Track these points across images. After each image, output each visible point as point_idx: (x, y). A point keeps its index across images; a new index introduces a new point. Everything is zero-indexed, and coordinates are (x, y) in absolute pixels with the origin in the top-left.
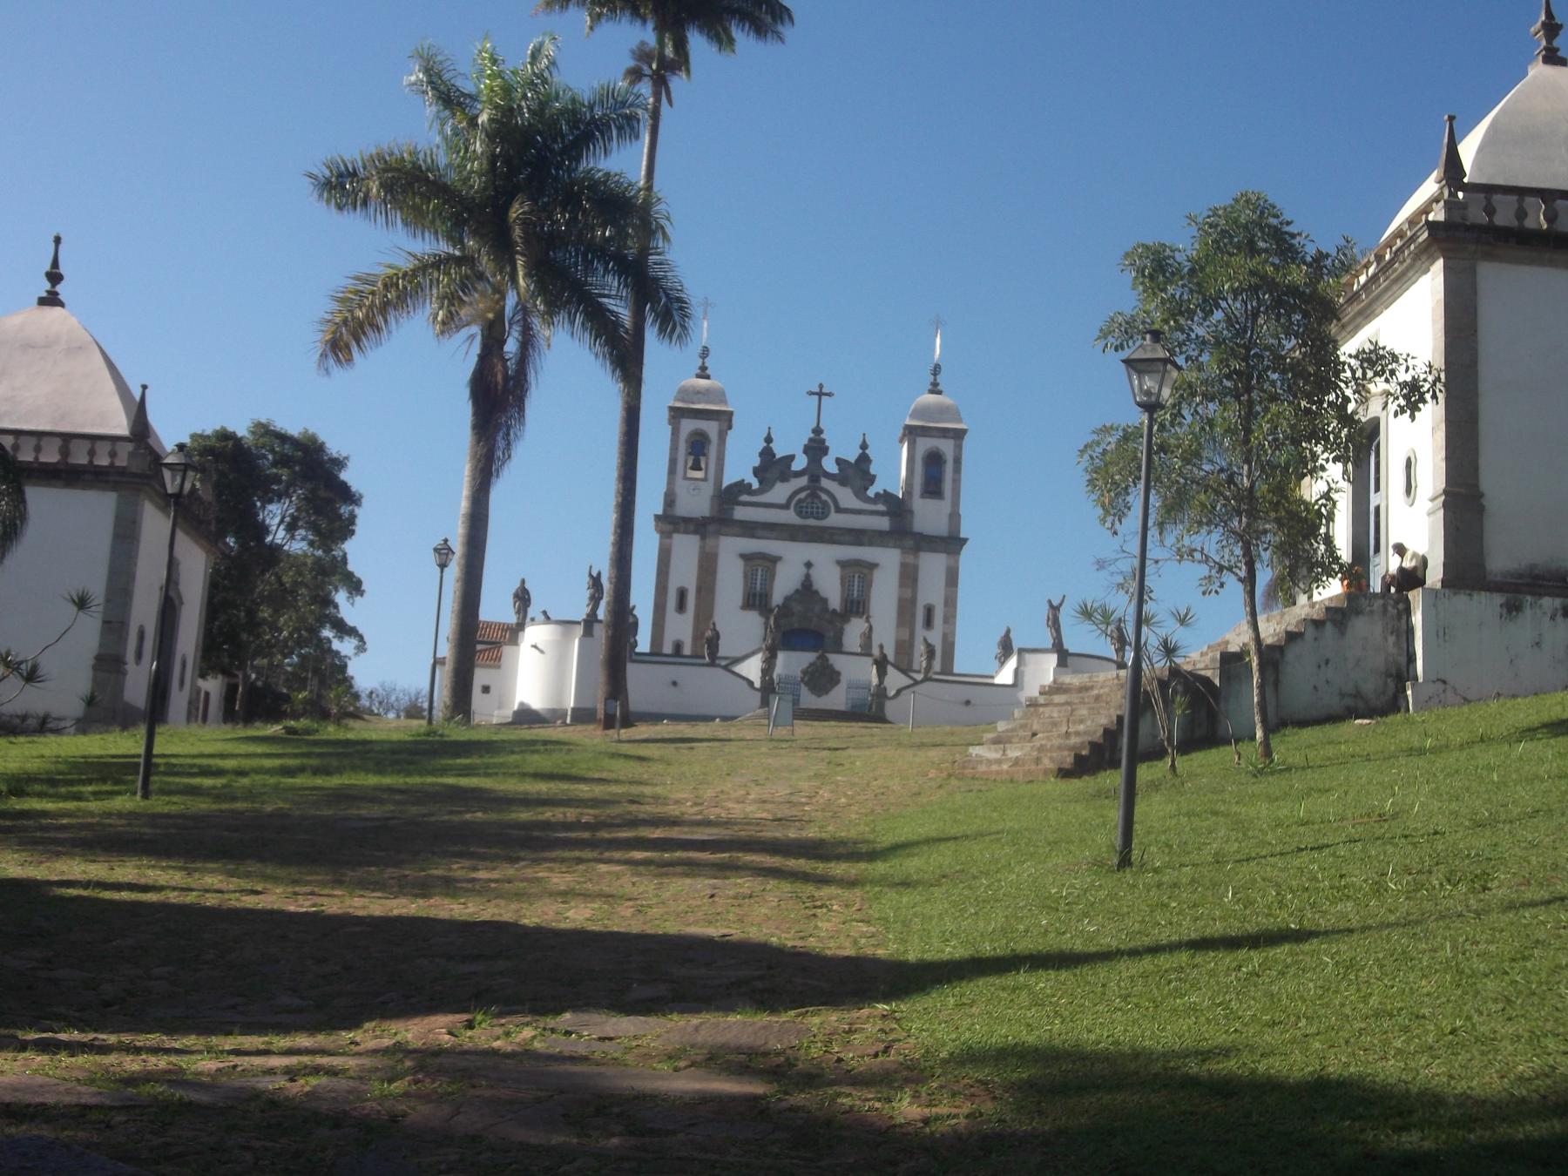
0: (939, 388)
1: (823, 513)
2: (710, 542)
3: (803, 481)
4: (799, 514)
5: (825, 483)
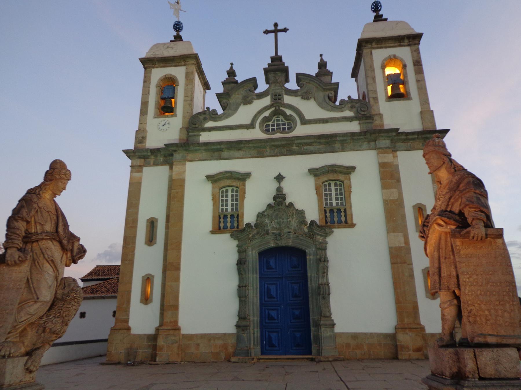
0: (384, 17)
1: (289, 128)
2: (176, 168)
3: (267, 101)
4: (267, 131)
5: (288, 99)
